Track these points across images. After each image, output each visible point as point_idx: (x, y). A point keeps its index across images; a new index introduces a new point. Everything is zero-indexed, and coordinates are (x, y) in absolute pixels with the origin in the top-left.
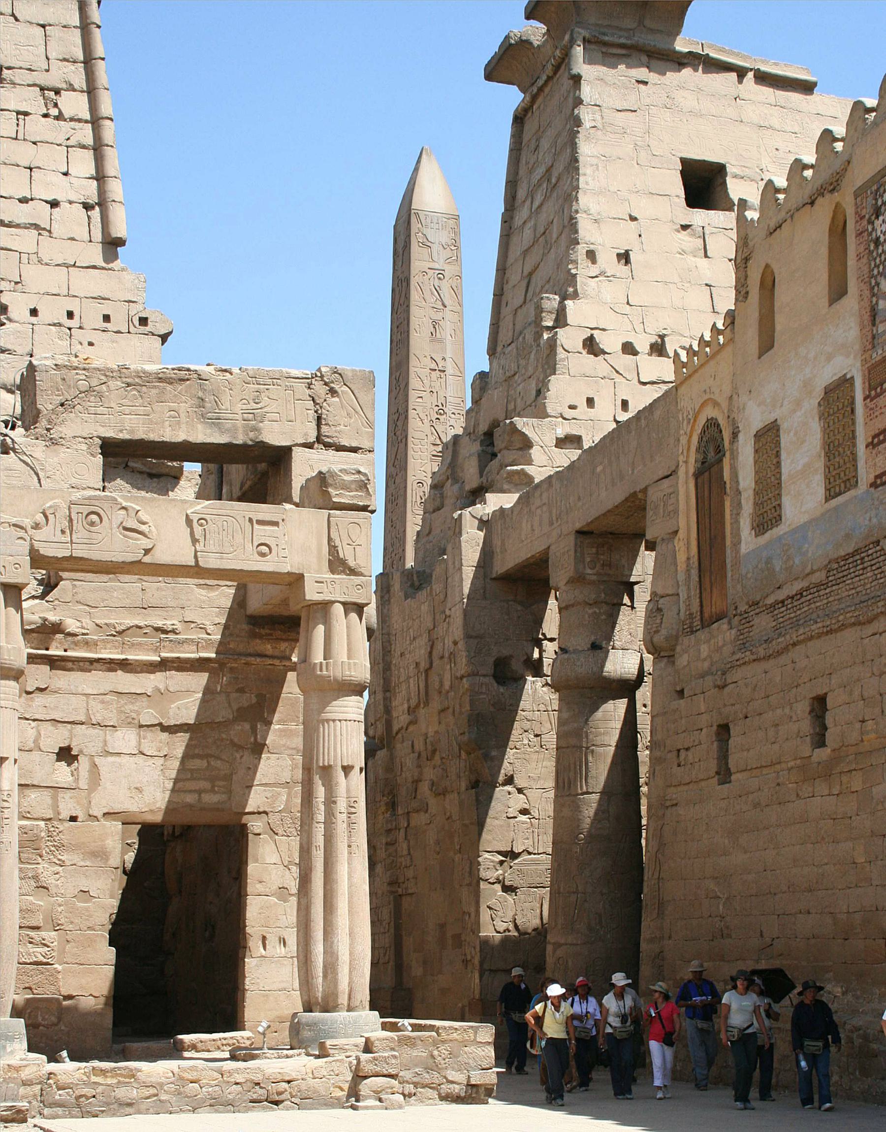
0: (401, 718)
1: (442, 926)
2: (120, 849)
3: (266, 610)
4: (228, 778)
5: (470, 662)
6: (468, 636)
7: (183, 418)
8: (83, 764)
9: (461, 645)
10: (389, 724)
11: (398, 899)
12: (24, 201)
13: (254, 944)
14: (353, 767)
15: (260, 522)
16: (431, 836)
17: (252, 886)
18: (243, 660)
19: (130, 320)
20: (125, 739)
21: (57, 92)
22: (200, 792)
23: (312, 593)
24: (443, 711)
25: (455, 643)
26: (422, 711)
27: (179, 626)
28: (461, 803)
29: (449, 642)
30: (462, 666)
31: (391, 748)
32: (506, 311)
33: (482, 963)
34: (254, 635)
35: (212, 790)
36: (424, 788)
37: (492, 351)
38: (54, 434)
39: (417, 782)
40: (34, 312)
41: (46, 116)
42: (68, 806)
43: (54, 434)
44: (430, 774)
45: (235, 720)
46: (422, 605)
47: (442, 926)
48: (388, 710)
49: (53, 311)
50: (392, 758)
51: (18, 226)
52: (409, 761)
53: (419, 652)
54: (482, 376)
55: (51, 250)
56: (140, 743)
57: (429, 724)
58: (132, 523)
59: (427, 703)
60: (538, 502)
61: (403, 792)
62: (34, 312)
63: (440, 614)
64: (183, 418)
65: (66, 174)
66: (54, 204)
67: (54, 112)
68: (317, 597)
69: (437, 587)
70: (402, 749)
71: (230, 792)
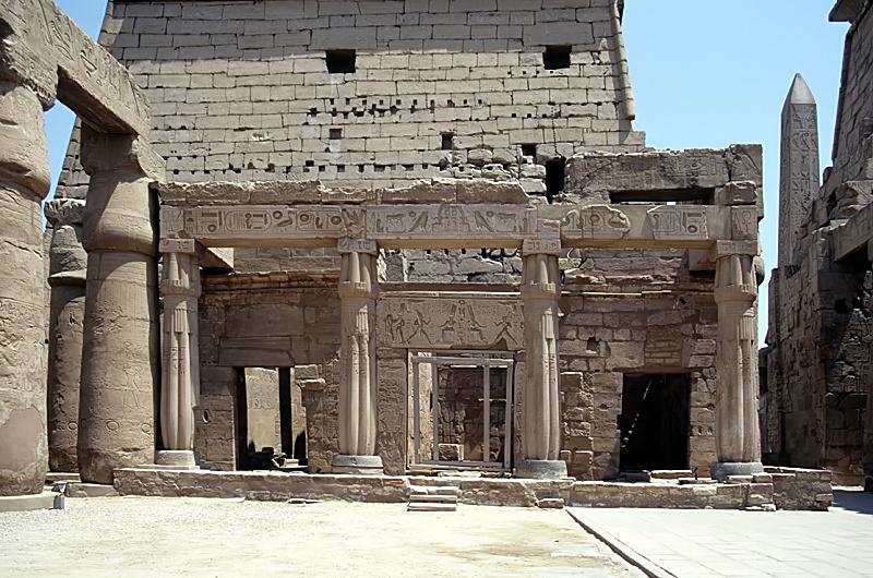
0: (784, 334)
1: (805, 427)
2: (618, 381)
3: (699, 267)
4: (680, 351)
5: (822, 302)
6: (820, 290)
7: (654, 178)
8: (602, 346)
9: (817, 295)
10: (779, 337)
11: (783, 415)
12: (584, 104)
13: (695, 431)
14: (747, 340)
15: (689, 215)
16: (800, 386)
17: (693, 403)
18: (688, 293)
20: (622, 335)
21: (599, 53)
22: (664, 358)
23: (721, 250)
24: (806, 328)
25: (813, 295)
26: (795, 330)
27: (652, 278)
28: (816, 370)
29: (810, 295)
30: (817, 305)
31: (780, 348)
32: (842, 136)
33: (827, 442)
34: (693, 281)
35: (671, 357)
36: (797, 365)
37: (834, 157)
38: (585, 190)
39: (793, 362)
41: (593, 64)
42: (593, 365)
43: (585, 190)
44: (799, 358)
45: (683, 323)
46: (796, 281)
47: (805, 427)
48: (778, 331)
50: (780, 352)
51: (582, 116)
52: (789, 353)
53: (794, 302)
54: (828, 170)
55: (597, 125)
56: (631, 335)
57: (799, 334)
58: (616, 219)
59: (798, 326)
60: (860, 220)
61: (786, 368)
63: (805, 284)
64: (654, 178)
65: (604, 89)
66: (599, 104)
67: (598, 62)
68: (725, 253)
69: (803, 271)
70: (785, 348)
71: (681, 358)
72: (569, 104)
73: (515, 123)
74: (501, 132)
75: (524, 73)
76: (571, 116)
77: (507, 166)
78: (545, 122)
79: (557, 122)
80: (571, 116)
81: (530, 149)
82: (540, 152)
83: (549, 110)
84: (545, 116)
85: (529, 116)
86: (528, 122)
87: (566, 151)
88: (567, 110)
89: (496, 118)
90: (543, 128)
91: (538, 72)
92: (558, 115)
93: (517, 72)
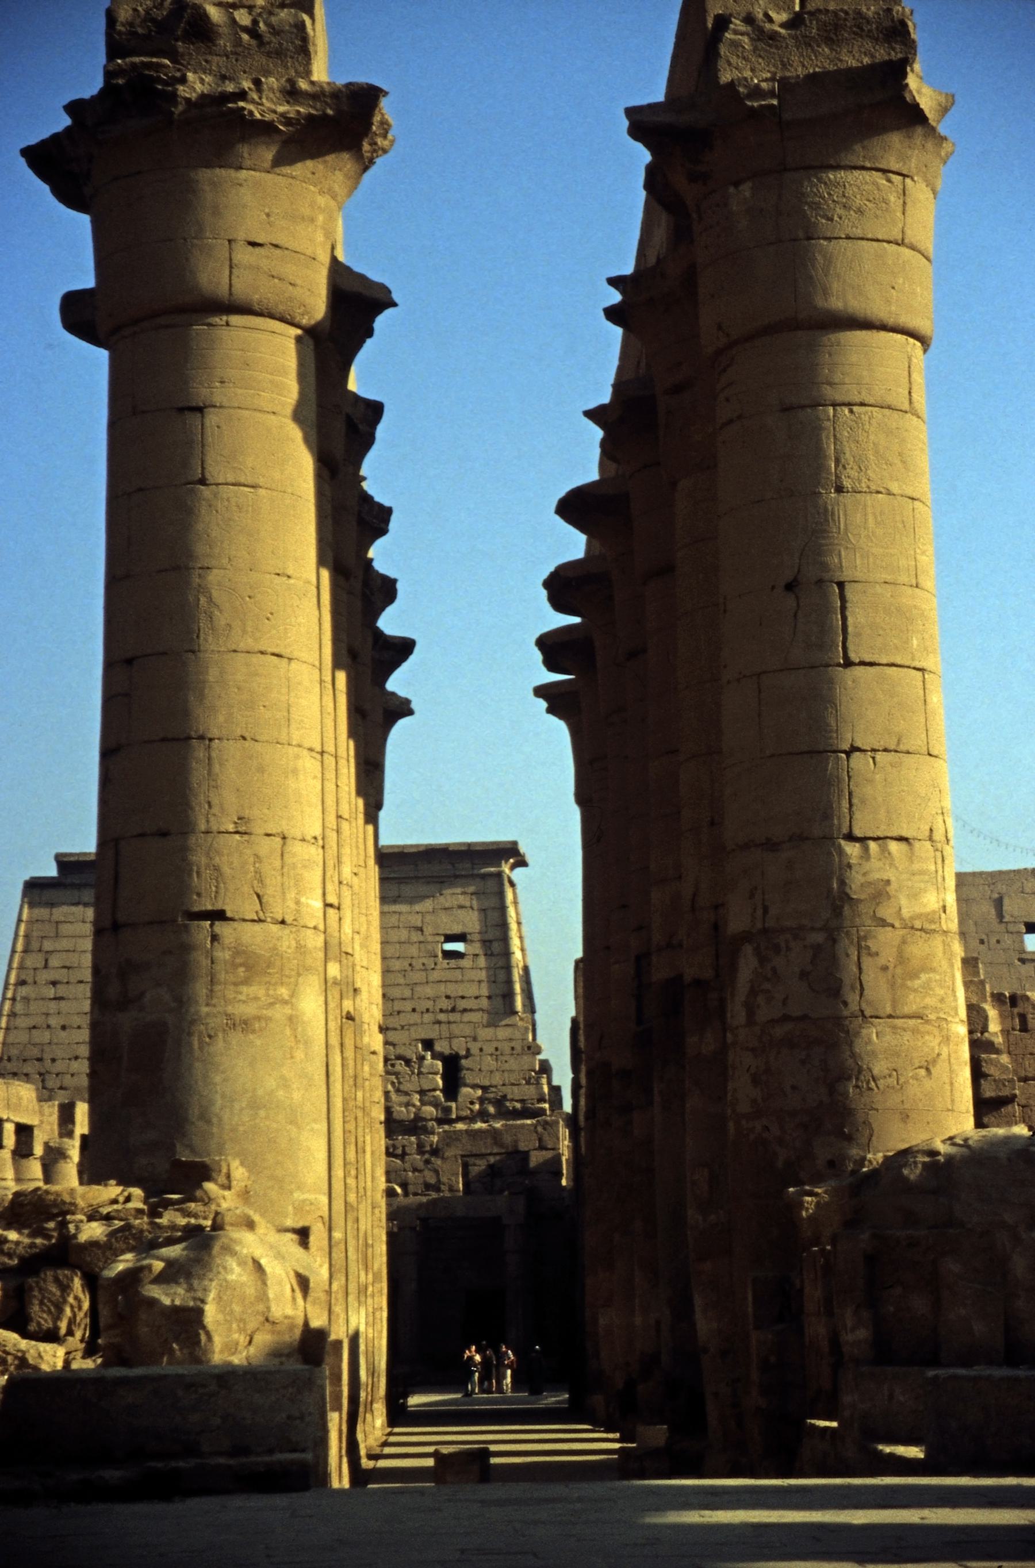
12: (476, 998)
19: (523, 1049)
40: (481, 1050)
49: (489, 1049)
62: (481, 1050)
67: (489, 952)
72: (463, 997)
73: (415, 1018)
74: (403, 1027)
75: (424, 964)
76: (465, 1010)
77: (408, 1062)
78: (442, 1017)
79: (453, 1017)
80: (465, 1010)
81: (428, 1044)
82: (438, 1047)
83: (445, 1004)
84: (441, 1011)
85: (428, 1010)
86: (428, 1018)
87: (459, 1046)
88: (462, 1004)
89: (399, 1012)
90: (439, 1022)
91: (436, 964)
92: (453, 1010)
93: (418, 964)
